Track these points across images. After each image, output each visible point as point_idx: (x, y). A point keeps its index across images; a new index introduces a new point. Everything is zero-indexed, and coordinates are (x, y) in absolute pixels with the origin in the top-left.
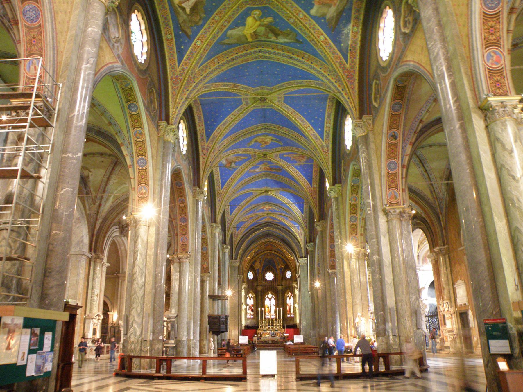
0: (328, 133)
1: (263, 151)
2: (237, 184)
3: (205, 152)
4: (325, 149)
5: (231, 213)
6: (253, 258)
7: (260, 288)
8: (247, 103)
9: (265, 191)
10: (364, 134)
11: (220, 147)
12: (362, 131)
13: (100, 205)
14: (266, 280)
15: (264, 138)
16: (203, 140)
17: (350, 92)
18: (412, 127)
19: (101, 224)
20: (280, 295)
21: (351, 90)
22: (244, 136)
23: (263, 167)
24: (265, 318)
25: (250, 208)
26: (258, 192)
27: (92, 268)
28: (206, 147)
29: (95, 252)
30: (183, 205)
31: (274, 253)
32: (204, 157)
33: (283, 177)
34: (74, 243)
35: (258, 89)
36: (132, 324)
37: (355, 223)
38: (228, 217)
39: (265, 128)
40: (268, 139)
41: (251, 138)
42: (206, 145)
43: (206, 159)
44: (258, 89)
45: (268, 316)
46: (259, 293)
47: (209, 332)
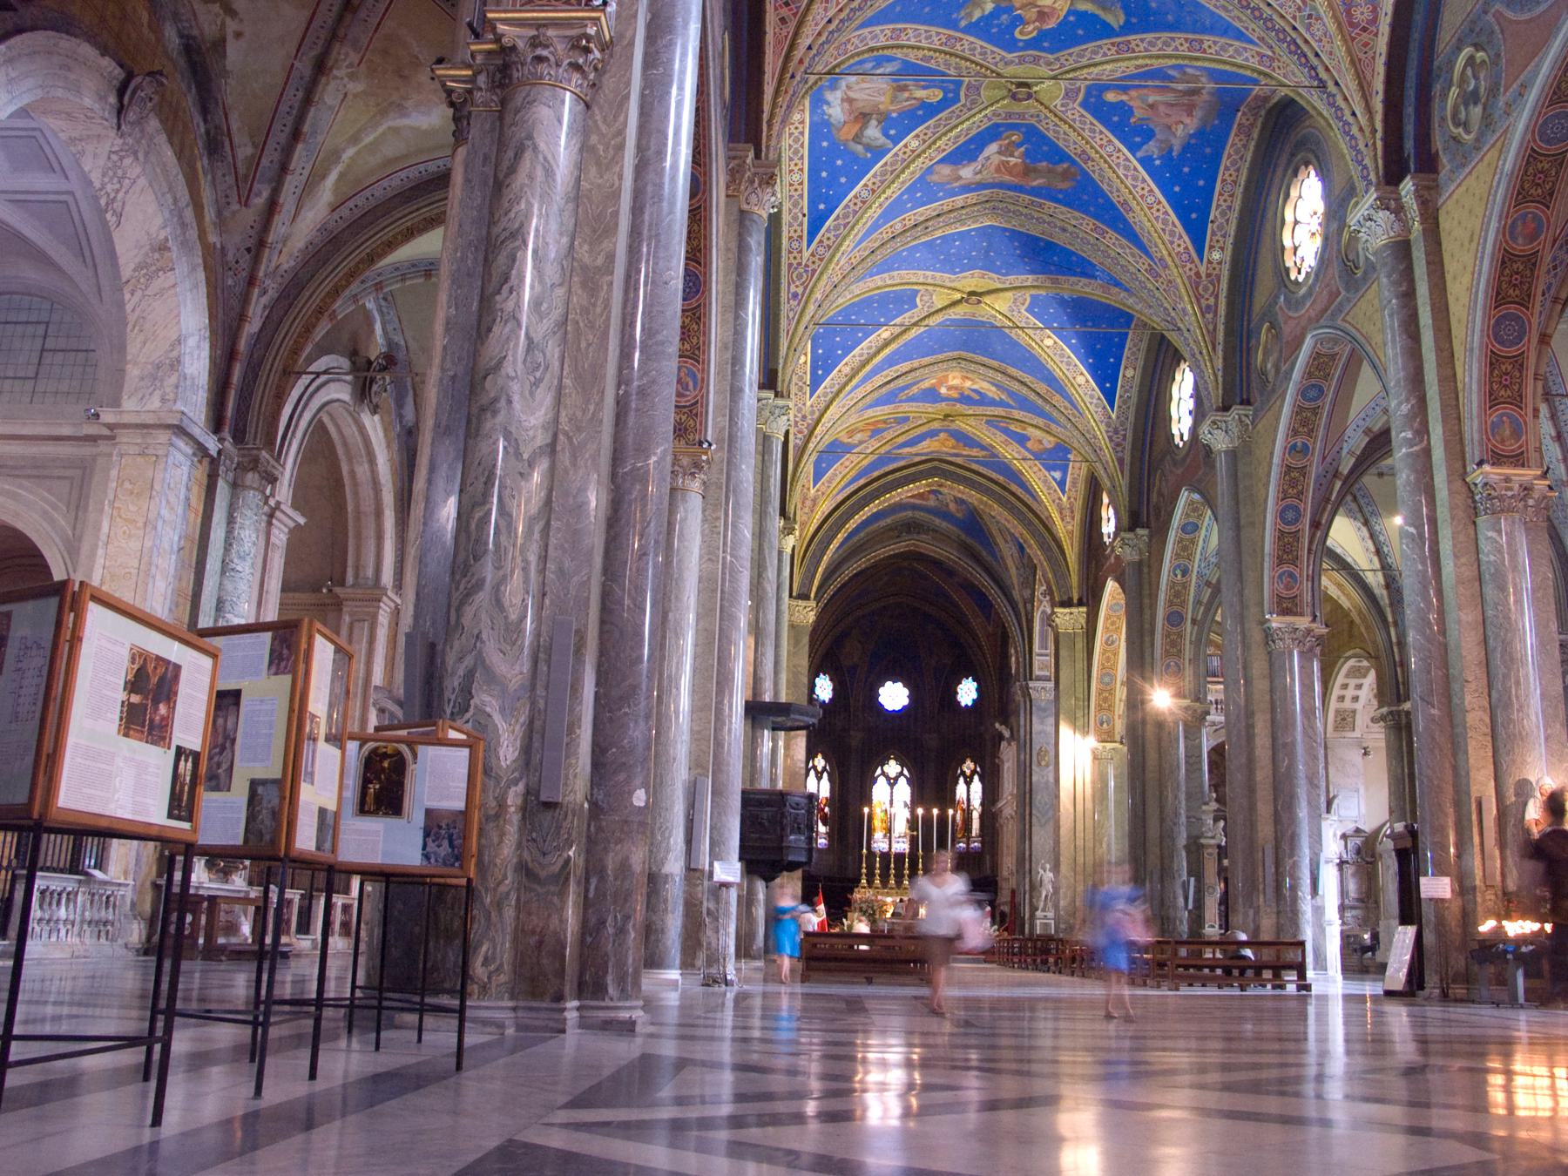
2: (876, 226)
5: (815, 383)
7: (856, 738)
9: (972, 293)
13: (272, 206)
19: (272, 307)
23: (996, 159)
24: (871, 854)
25: (891, 373)
27: (219, 516)
29: (239, 436)
32: (784, 12)
33: (1070, 216)
34: (133, 372)
36: (467, 692)
37: (1513, 351)
45: (880, 844)
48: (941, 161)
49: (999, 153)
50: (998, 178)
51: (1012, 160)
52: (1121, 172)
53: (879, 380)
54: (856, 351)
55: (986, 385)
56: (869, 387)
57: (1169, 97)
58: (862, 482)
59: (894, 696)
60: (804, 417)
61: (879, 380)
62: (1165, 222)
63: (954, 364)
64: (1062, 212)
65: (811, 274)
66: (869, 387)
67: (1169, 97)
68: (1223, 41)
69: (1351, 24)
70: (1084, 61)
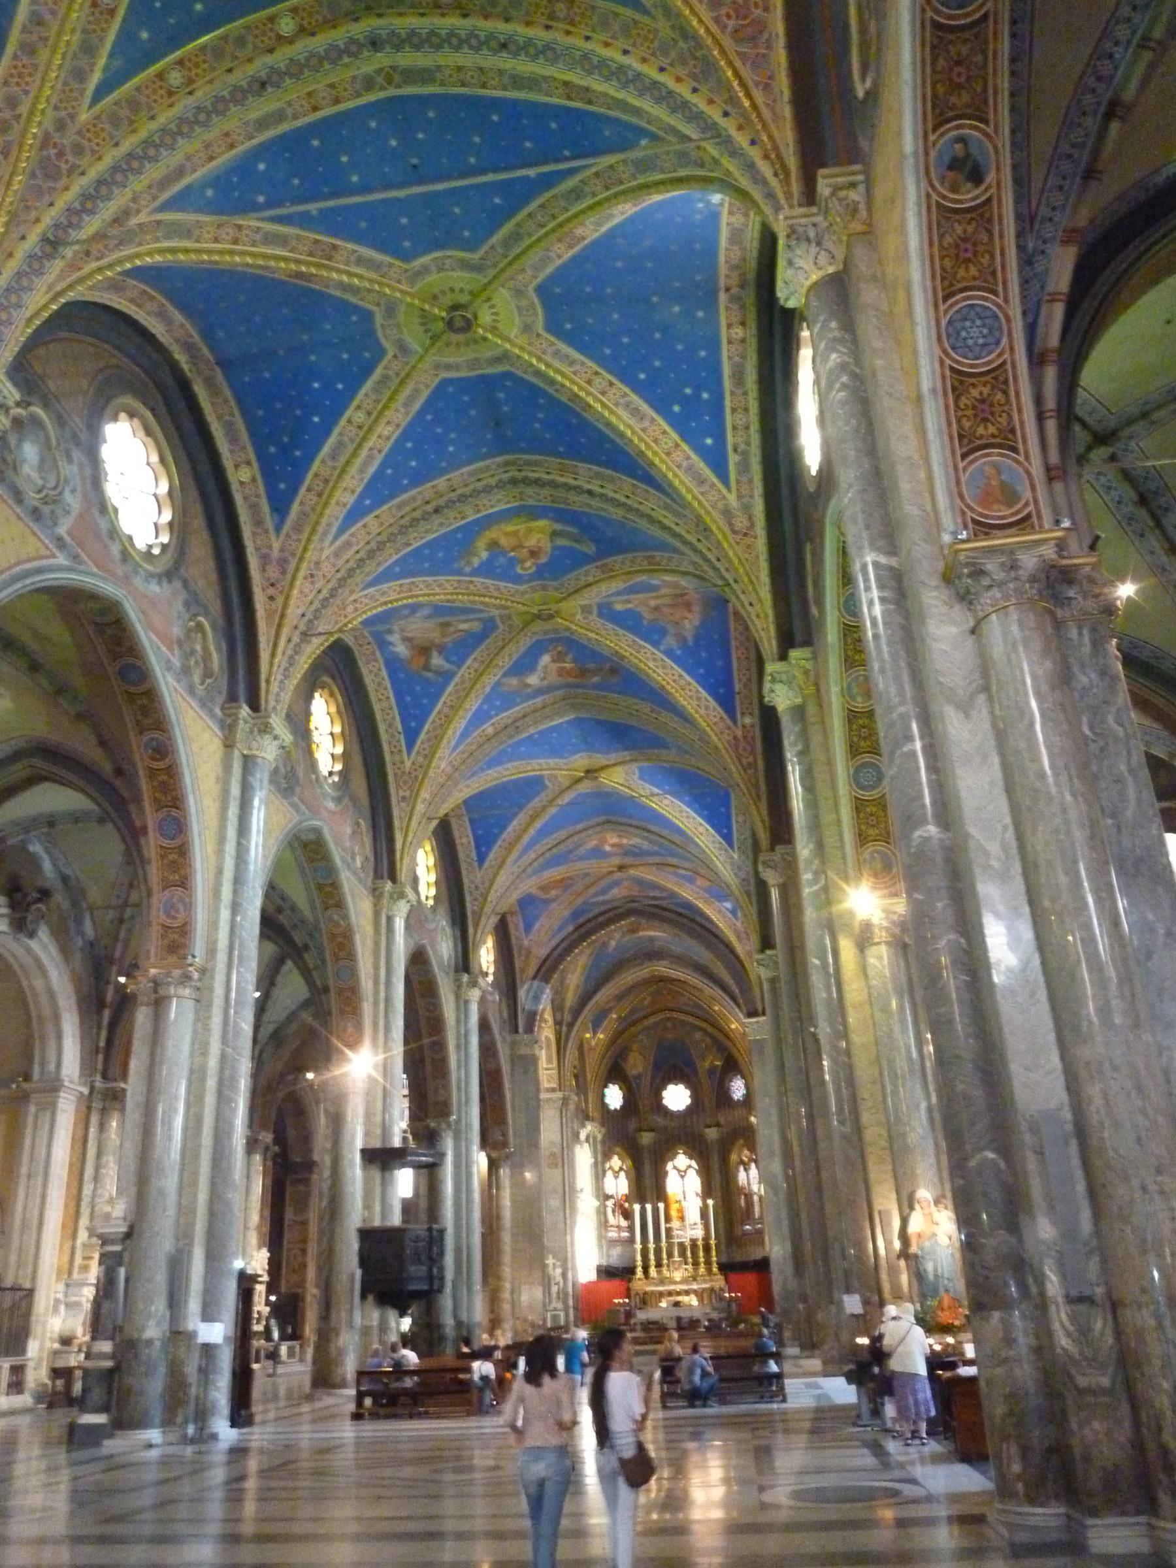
0: (745, 455)
1: (534, 590)
4: (741, 522)
5: (481, 858)
6: (613, 1041)
8: (403, 348)
9: (588, 772)
10: (831, 270)
11: (337, 555)
12: (823, 259)
15: (522, 527)
17: (754, 106)
18: (1065, 148)
21: (759, 98)
22: (437, 520)
23: (554, 667)
25: (550, 841)
26: (563, 777)
28: (275, 553)
30: (161, 765)
31: (682, 1017)
32: (271, 591)
35: (425, 270)
39: (514, 481)
41: (471, 531)
42: (276, 545)
43: (280, 601)
44: (425, 270)
46: (646, 1155)
47: (363, 1297)
48: (504, 675)
49: (554, 661)
53: (540, 847)
54: (510, 829)
55: (638, 840)
60: (477, 888)
62: (699, 699)
65: (415, 780)
66: (532, 855)
69: (734, 532)
70: (582, 583)
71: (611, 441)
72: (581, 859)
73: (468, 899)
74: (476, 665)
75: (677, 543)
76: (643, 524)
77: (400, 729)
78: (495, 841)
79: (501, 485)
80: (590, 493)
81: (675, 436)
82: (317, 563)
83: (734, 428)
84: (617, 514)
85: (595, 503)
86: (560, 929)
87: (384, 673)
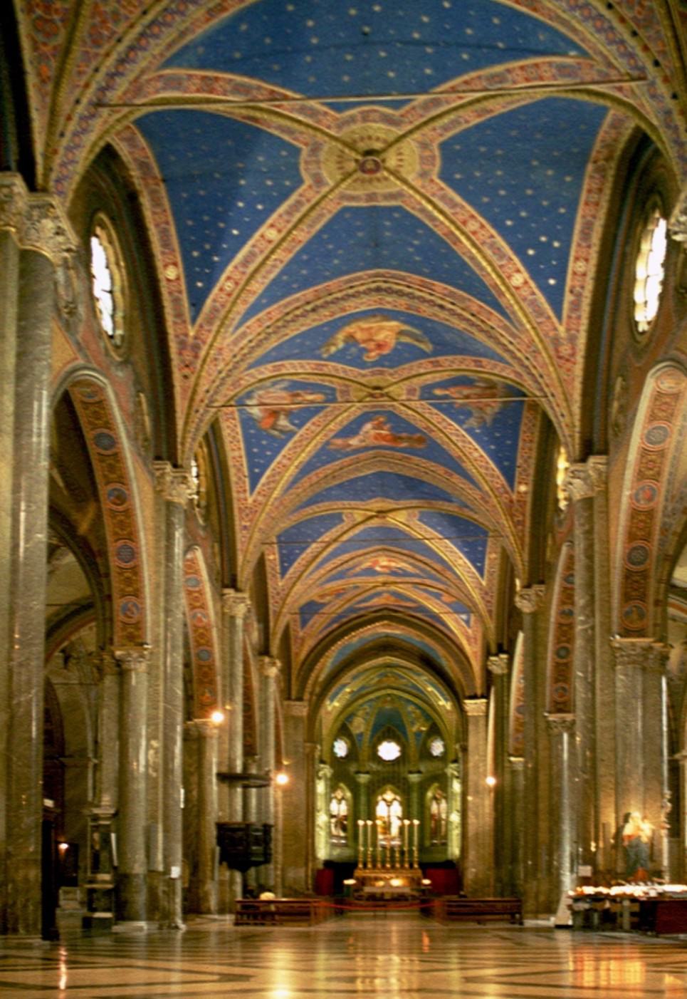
0: (579, 295)
3: (188, 356)
5: (284, 571)
7: (363, 779)
9: (379, 512)
11: (235, 343)
14: (380, 760)
16: (179, 315)
20: (415, 796)
22: (313, 316)
23: (373, 432)
26: (359, 516)
33: (431, 465)
38: (276, 584)
39: (378, 290)
40: (387, 332)
42: (192, 333)
46: (363, 791)
49: (374, 428)
50: (377, 443)
51: (383, 432)
52: (454, 438)
53: (329, 566)
54: (309, 550)
56: (322, 571)
57: (477, 391)
58: (335, 626)
59: (389, 751)
60: (278, 594)
61: (329, 566)
63: (380, 553)
64: (424, 462)
66: (322, 571)
67: (477, 391)
68: (493, 362)
70: (414, 373)
71: (473, 273)
72: (356, 575)
73: (271, 601)
74: (313, 428)
75: (506, 356)
76: (481, 337)
77: (246, 474)
78: (294, 560)
79: (366, 292)
80: (442, 307)
81: (526, 275)
82: (221, 349)
83: (575, 273)
84: (462, 325)
85: (443, 314)
86: (330, 624)
87: (239, 430)
